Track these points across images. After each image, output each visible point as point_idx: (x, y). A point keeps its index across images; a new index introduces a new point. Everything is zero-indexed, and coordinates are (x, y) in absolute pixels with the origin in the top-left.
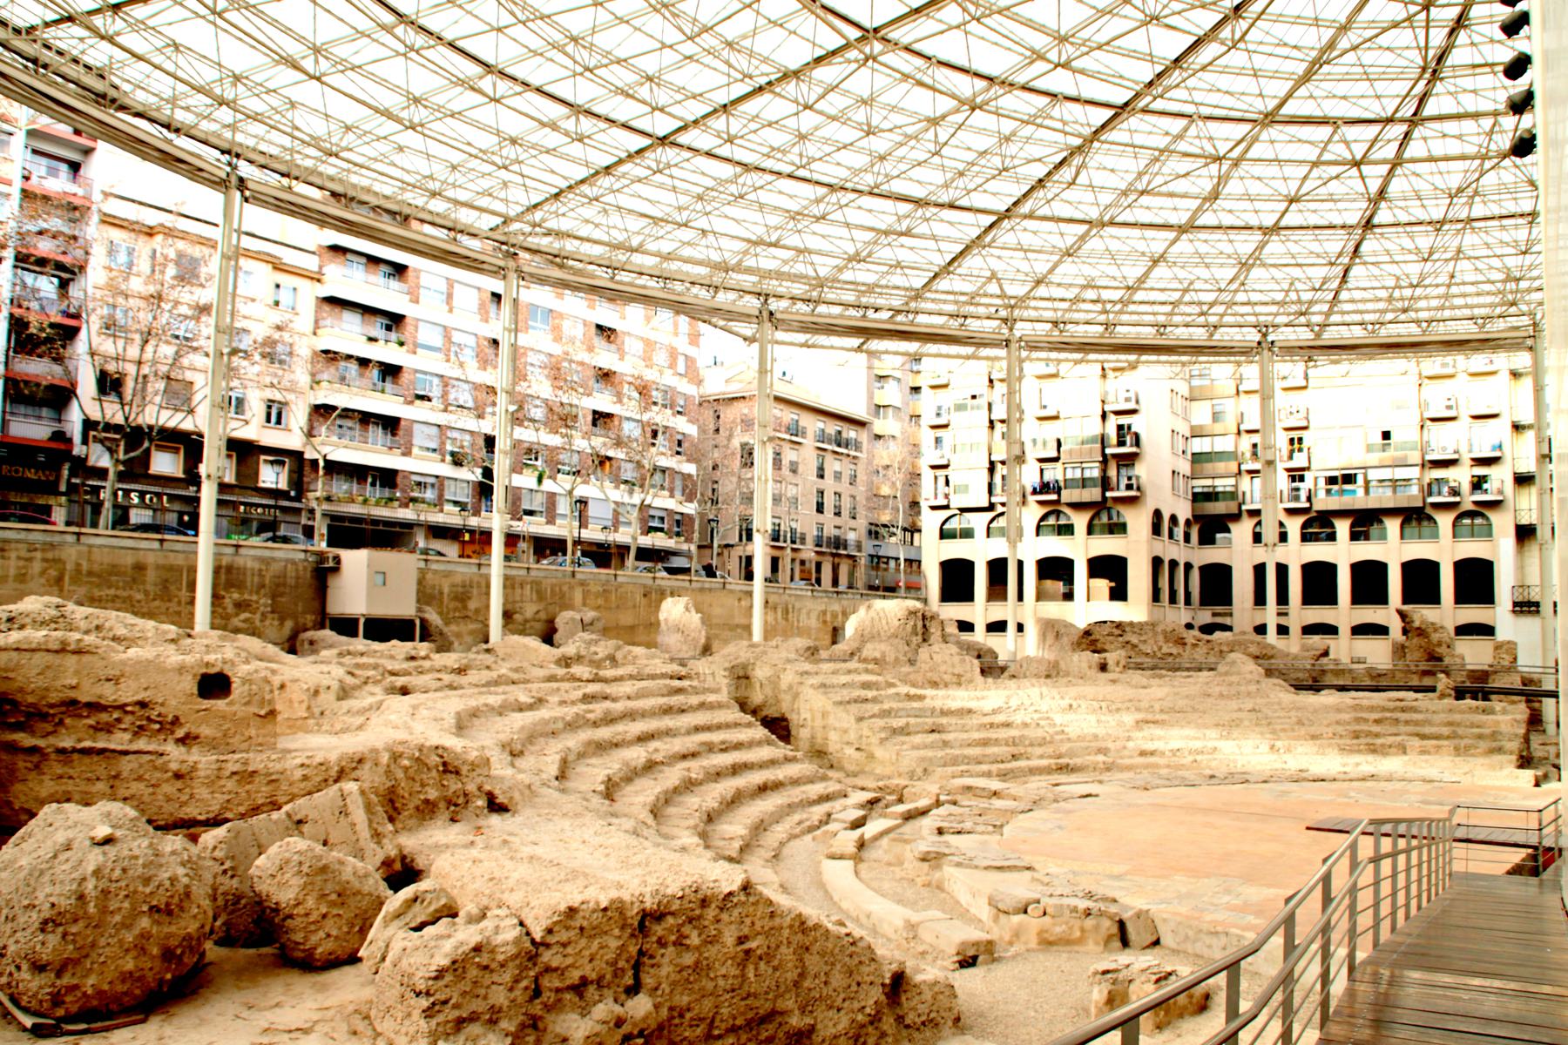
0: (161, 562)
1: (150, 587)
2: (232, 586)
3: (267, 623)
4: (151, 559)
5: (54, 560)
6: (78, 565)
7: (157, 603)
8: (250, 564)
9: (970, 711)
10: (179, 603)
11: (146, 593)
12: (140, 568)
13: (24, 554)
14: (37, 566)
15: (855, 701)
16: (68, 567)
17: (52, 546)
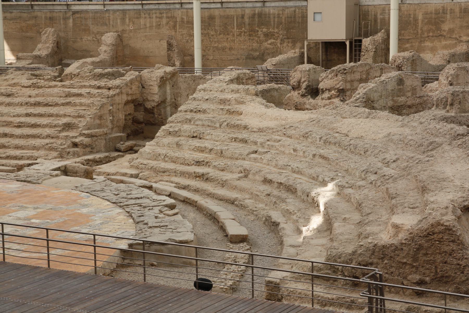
0: (222, 14)
1: (217, 28)
2: (262, 24)
3: (285, 45)
4: (217, 13)
5: (171, 17)
6: (182, 18)
7: (222, 36)
8: (272, 11)
9: (245, 127)
10: (234, 35)
11: (216, 31)
12: (212, 18)
13: (158, 15)
14: (164, 21)
15: (191, 111)
16: (178, 20)
17: (170, 9)
